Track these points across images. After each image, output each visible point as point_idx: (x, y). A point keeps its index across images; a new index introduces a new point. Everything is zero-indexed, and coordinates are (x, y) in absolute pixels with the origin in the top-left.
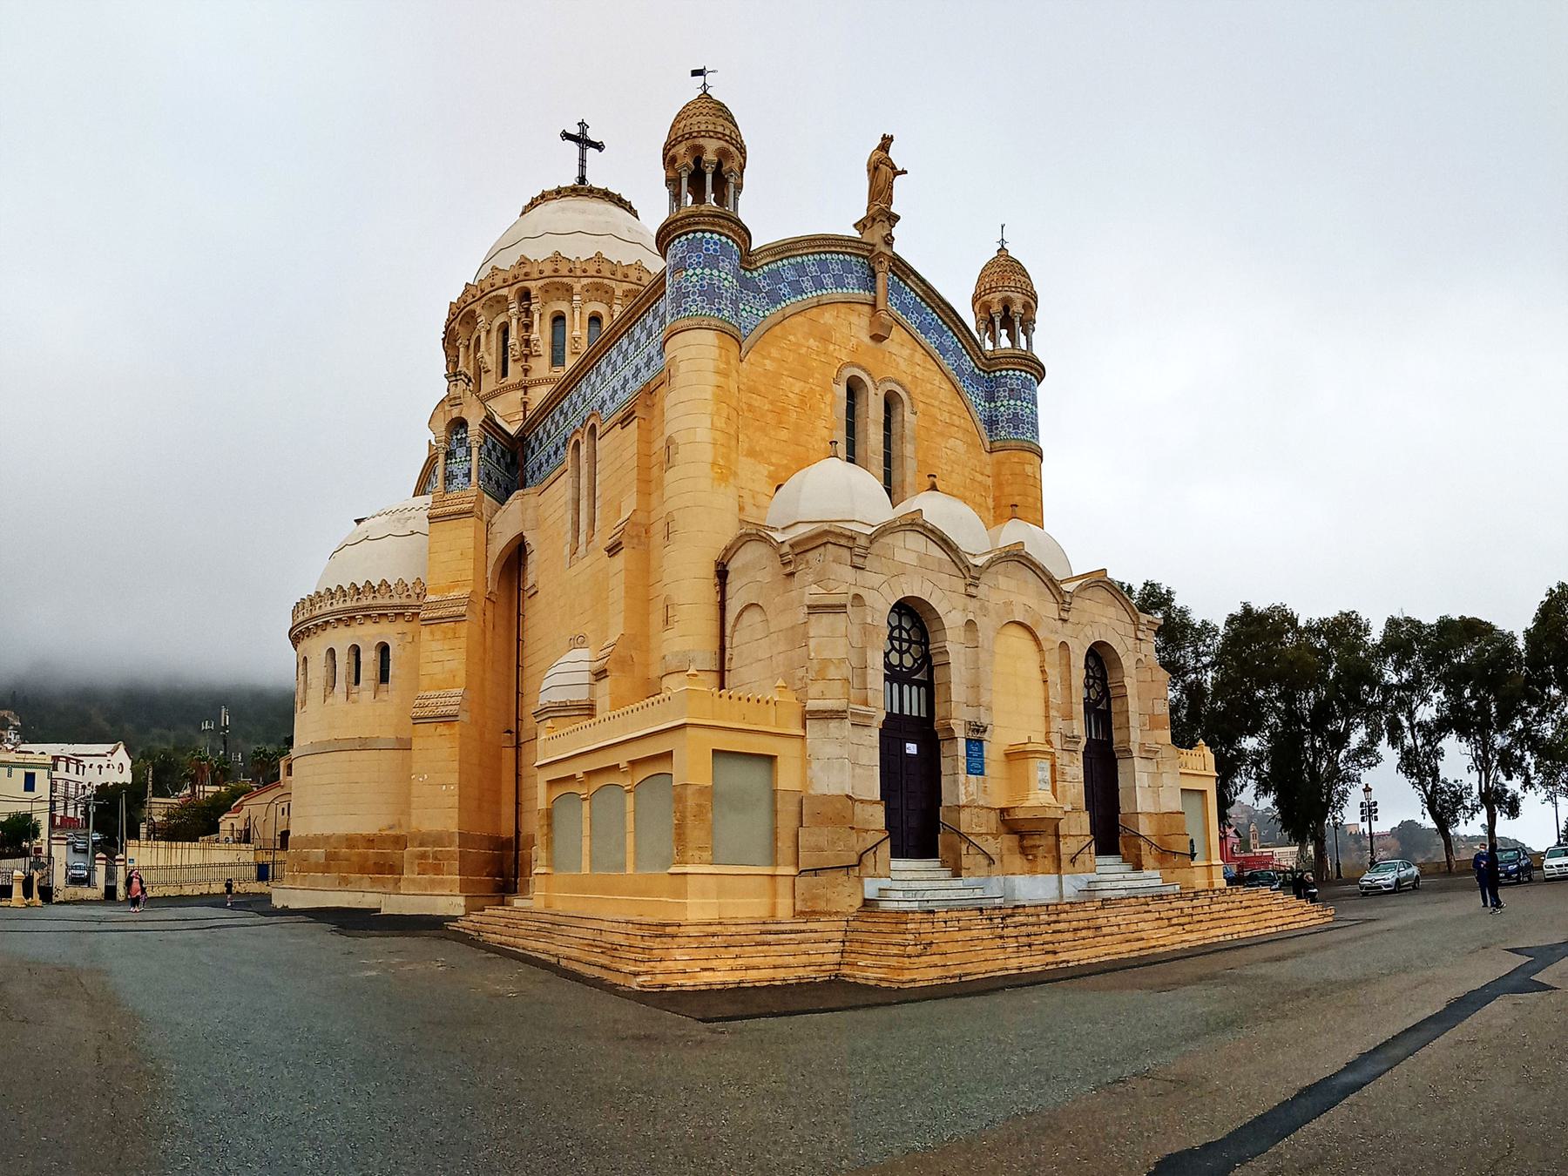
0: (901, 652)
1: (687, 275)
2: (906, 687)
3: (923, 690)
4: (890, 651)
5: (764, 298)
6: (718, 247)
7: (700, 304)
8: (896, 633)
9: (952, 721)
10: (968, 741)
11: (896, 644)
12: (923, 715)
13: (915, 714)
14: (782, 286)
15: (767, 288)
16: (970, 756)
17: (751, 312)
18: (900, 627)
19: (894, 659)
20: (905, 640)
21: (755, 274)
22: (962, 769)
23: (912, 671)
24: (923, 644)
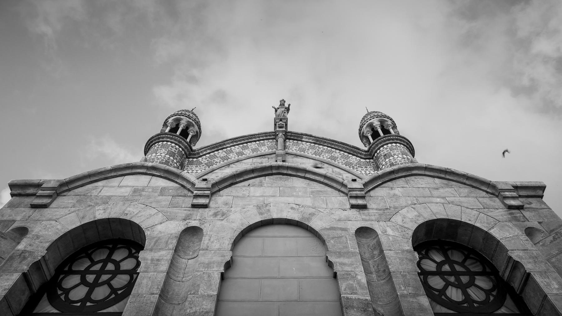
11: (105, 277)
21: (200, 159)
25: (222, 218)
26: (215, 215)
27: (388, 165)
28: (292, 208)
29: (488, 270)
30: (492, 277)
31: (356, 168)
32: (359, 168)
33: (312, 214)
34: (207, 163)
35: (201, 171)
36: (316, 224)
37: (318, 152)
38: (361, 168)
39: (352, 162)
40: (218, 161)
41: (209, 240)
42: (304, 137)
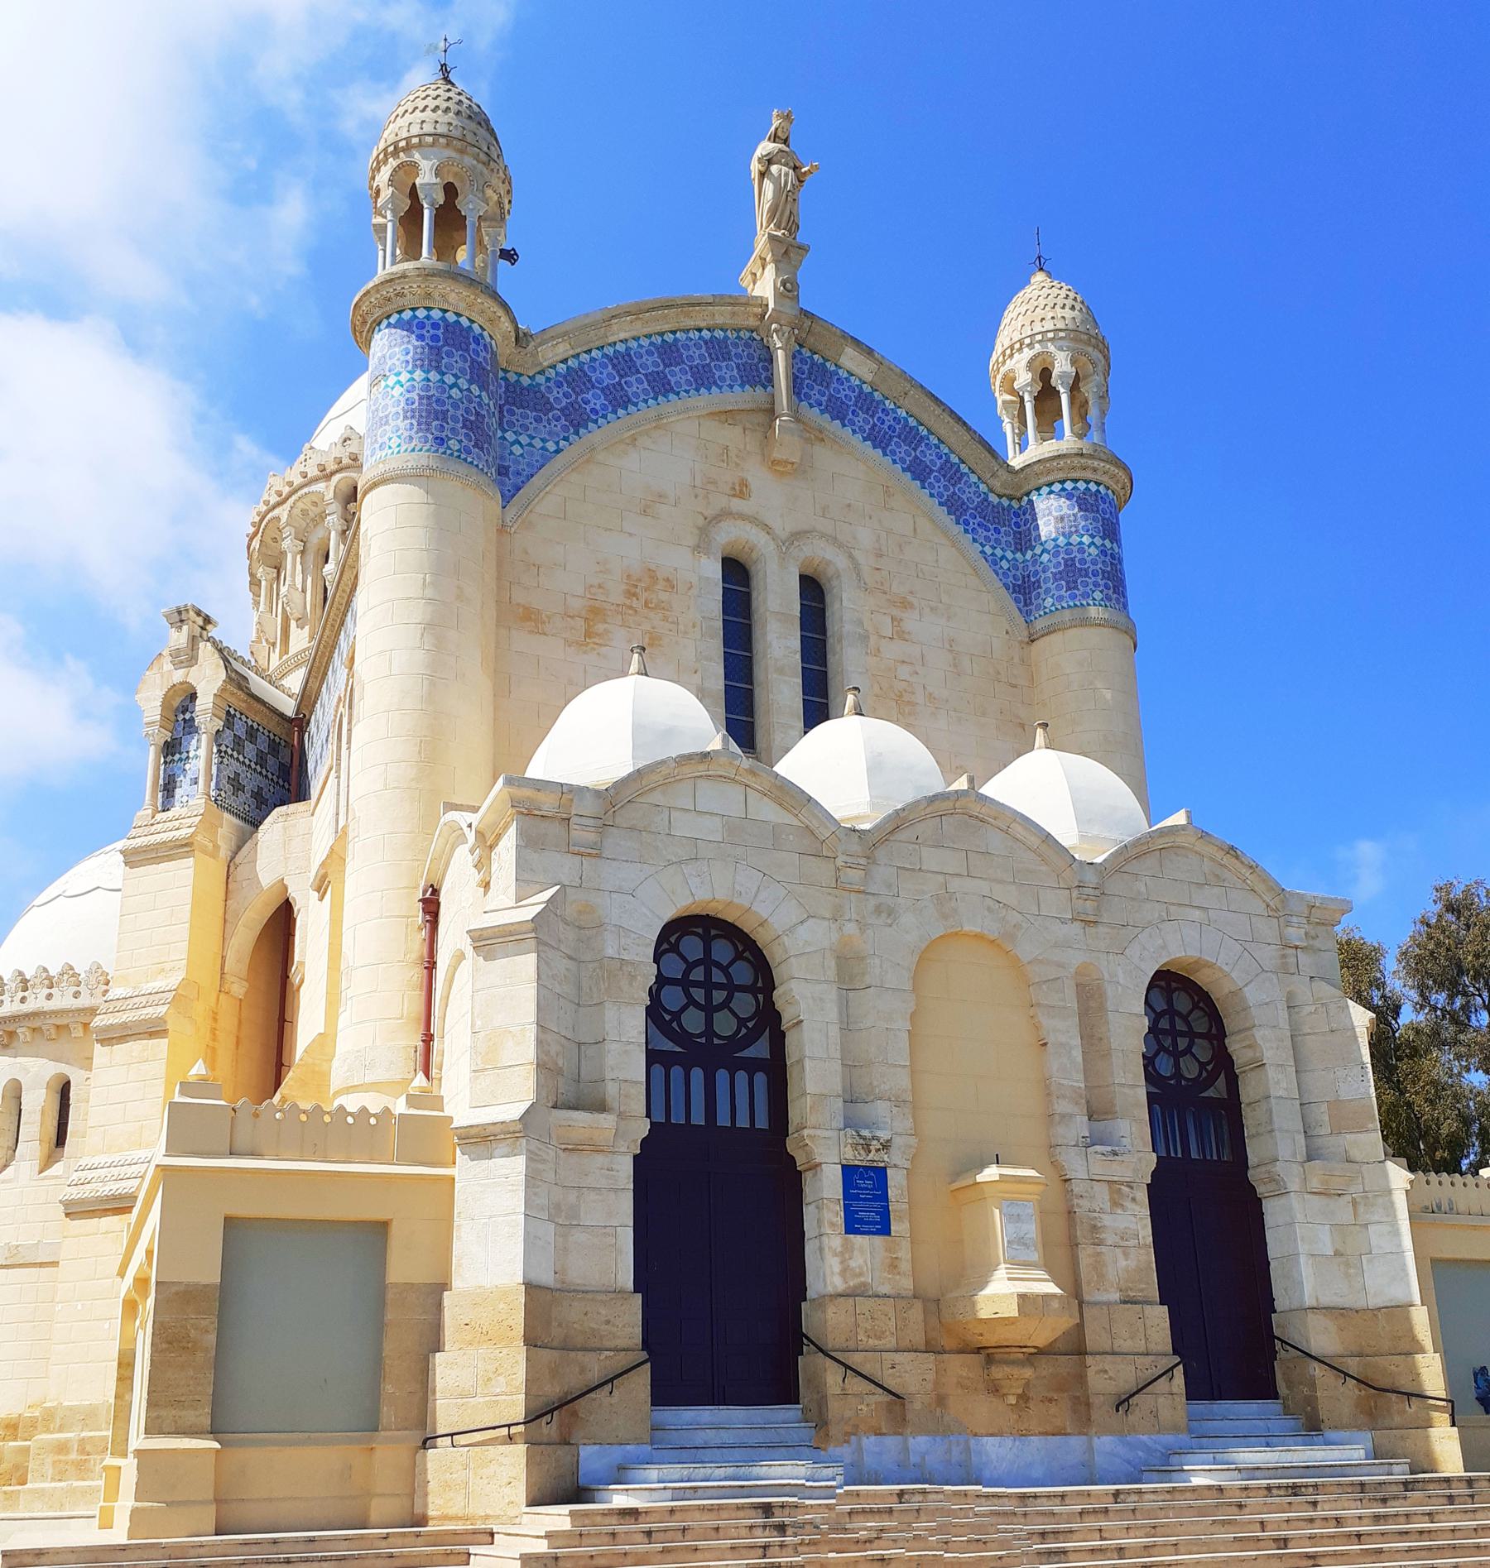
0: (1176, 1055)
1: (387, 386)
2: (722, 1076)
3: (760, 1079)
4: (684, 1009)
5: (558, 419)
6: (440, 333)
7: (406, 434)
8: (1164, 1024)
9: (806, 1132)
10: (849, 1171)
12: (762, 1123)
13: (743, 1122)
14: (589, 396)
15: (565, 401)
16: (857, 1197)
17: (530, 445)
18: (1171, 1012)
19: (1165, 1066)
20: (1182, 1034)
22: (832, 1224)
23: (737, 1042)
24: (760, 990)
25: (889, 921)
26: (878, 910)
27: (1060, 559)
28: (989, 909)
29: (1214, 1031)
30: (1215, 1042)
31: (973, 529)
32: (980, 530)
33: (1017, 926)
34: (566, 408)
35: (557, 443)
36: (1026, 950)
37: (879, 432)
38: (985, 533)
39: (964, 497)
40: (598, 407)
41: (881, 967)
42: (850, 351)
